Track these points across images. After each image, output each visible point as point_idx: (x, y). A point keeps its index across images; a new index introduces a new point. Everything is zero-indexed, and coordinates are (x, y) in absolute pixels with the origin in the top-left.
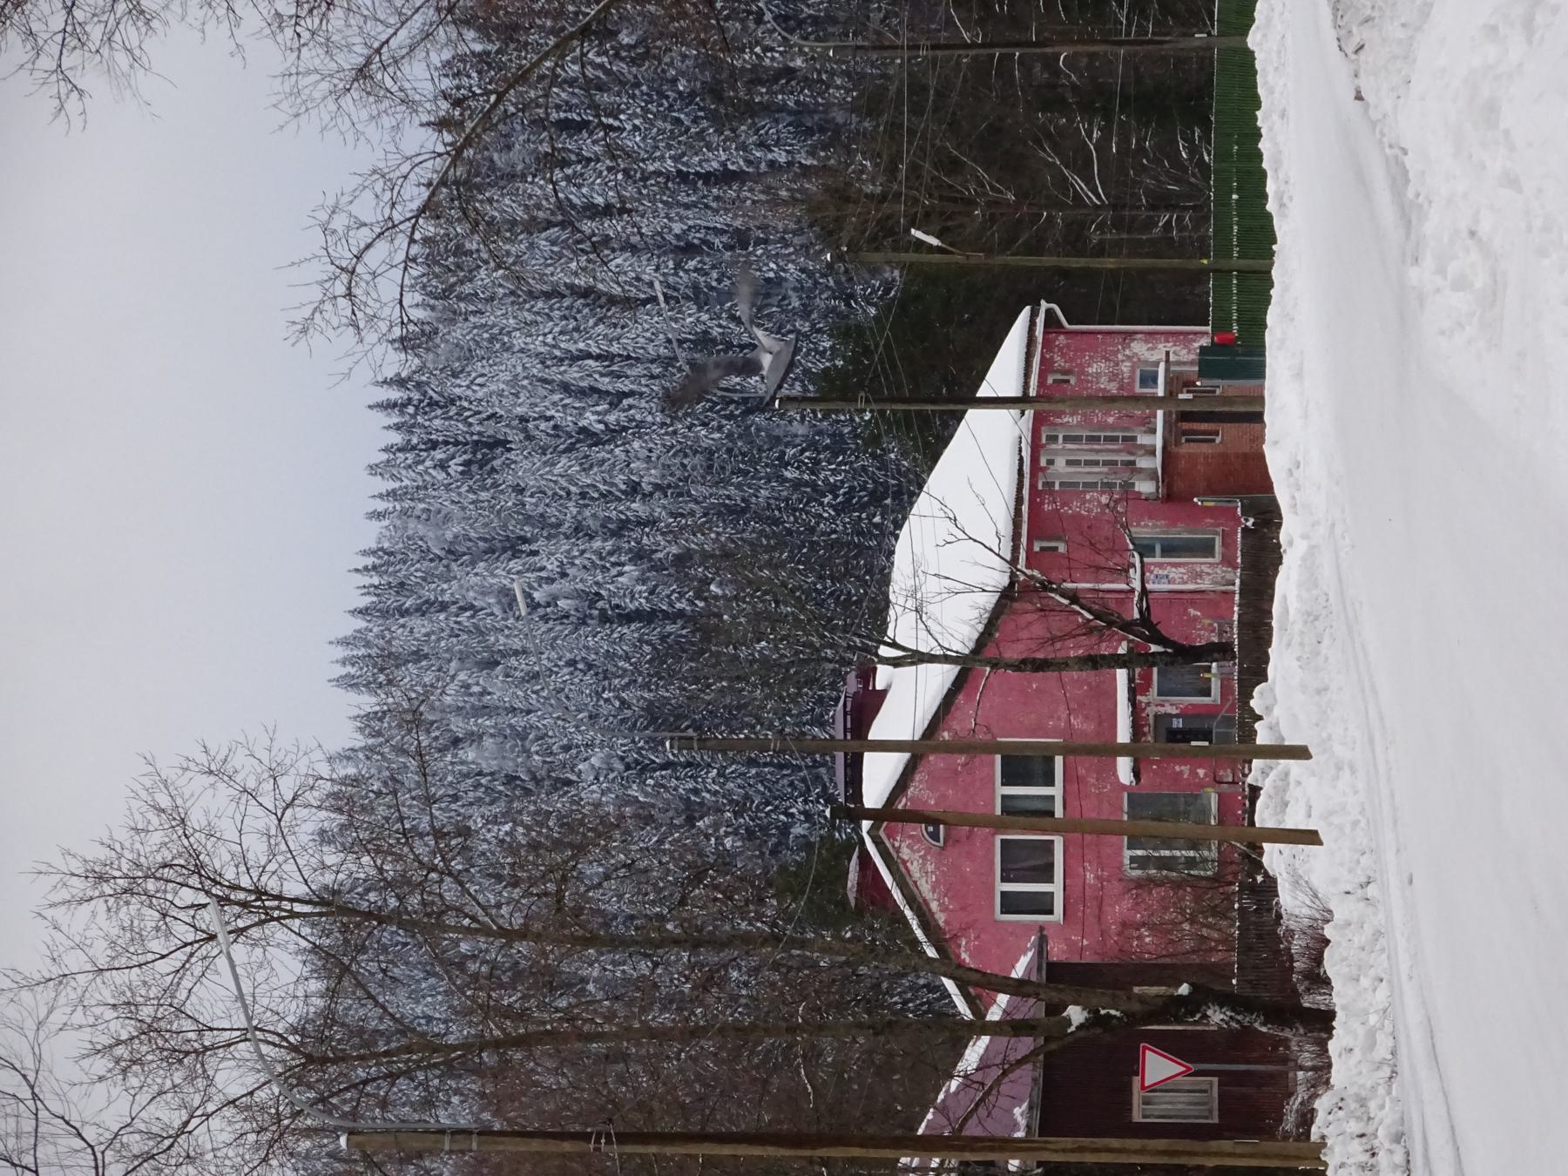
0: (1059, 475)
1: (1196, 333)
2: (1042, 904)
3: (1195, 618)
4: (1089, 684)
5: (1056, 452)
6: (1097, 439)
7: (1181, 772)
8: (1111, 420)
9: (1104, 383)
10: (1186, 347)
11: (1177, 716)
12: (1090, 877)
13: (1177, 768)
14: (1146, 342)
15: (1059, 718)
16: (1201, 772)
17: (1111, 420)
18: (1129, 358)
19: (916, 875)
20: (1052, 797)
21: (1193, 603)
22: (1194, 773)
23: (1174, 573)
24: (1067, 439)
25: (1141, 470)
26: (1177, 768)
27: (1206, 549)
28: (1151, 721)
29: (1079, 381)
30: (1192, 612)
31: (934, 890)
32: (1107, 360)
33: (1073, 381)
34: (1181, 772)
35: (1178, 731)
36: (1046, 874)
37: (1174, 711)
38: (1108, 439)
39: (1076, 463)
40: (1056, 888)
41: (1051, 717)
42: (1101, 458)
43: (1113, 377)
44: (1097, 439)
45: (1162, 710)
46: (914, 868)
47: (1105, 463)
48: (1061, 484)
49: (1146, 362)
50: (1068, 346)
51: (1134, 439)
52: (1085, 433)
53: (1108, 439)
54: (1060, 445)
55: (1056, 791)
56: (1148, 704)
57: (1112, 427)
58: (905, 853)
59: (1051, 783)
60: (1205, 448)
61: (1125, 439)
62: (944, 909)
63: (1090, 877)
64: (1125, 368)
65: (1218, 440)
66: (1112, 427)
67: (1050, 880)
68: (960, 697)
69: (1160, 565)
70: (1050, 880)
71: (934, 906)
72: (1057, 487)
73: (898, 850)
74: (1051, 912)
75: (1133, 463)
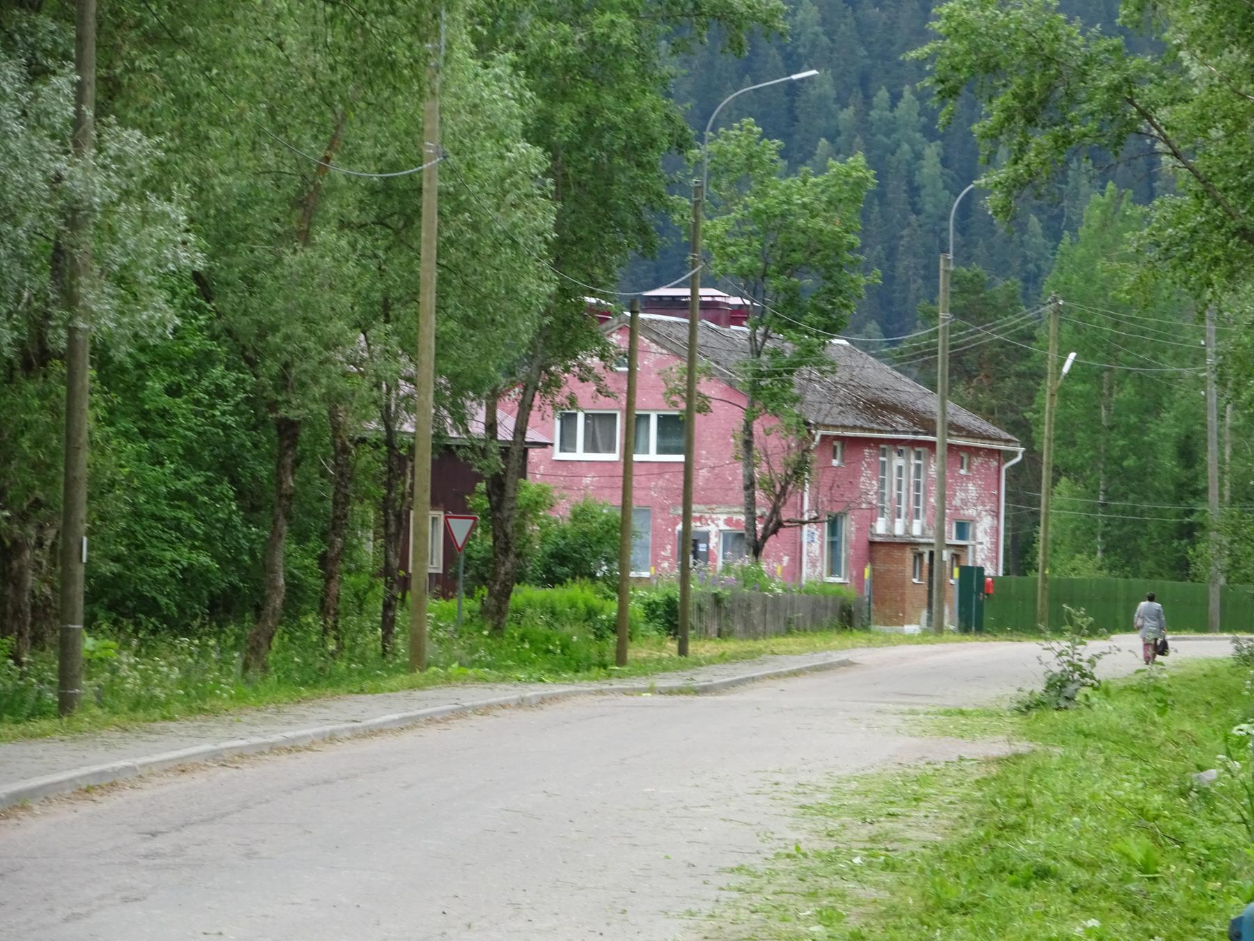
0: (890, 462)
1: (997, 565)
2: (567, 443)
3: (780, 561)
5: (909, 459)
6: (918, 489)
7: (664, 549)
8: (932, 500)
9: (960, 495)
10: (987, 558)
11: (708, 547)
12: (587, 481)
13: (669, 547)
14: (992, 527)
16: (666, 565)
17: (932, 500)
18: (979, 515)
20: (648, 452)
21: (792, 560)
22: (665, 558)
23: (816, 547)
24: (918, 467)
25: (893, 522)
26: (669, 547)
27: (833, 570)
28: (705, 529)
29: (962, 476)
30: (786, 559)
32: (978, 499)
33: (963, 472)
34: (664, 549)
36: (591, 446)
37: (711, 546)
38: (917, 497)
39: (900, 474)
40: (580, 454)
41: (708, 453)
42: (903, 493)
43: (965, 502)
44: (918, 489)
47: (899, 496)
48: (884, 462)
49: (975, 528)
50: (989, 468)
51: (918, 518)
52: (922, 480)
53: (917, 497)
54: (913, 461)
55: (653, 456)
57: (926, 501)
59: (661, 450)
60: (909, 570)
61: (918, 510)
63: (587, 481)
64: (971, 512)
65: (915, 580)
66: (926, 501)
67: (586, 450)
69: (821, 536)
70: (586, 450)
72: (882, 459)
74: (562, 450)
75: (899, 517)
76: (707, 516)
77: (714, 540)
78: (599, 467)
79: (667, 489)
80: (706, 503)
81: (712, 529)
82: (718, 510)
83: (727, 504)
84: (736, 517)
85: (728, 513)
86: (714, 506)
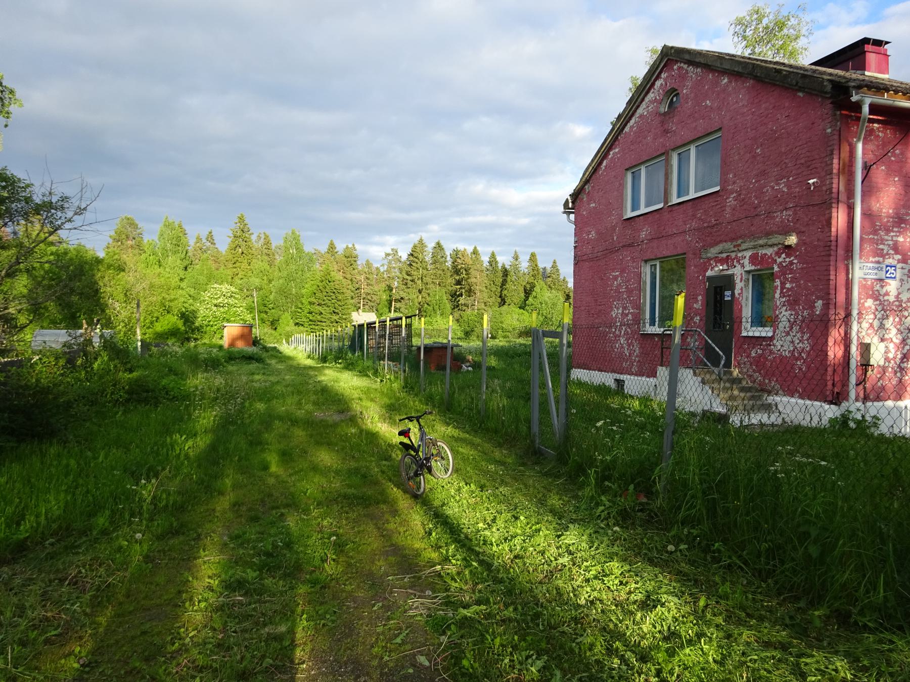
3: (812, 307)
4: (758, 206)
11: (733, 295)
12: (643, 235)
13: (700, 298)
15: (734, 183)
16: (697, 319)
19: (647, 100)
21: (826, 306)
26: (700, 298)
28: (730, 272)
30: (819, 304)
31: (641, 116)
35: (723, 296)
37: (737, 292)
40: (643, 210)
41: (735, 176)
45: (738, 281)
46: (651, 96)
56: (743, 266)
58: (658, 83)
62: (632, 127)
63: (643, 235)
68: (752, 81)
71: (632, 122)
73: (658, 77)
76: (733, 255)
77: (739, 285)
78: (650, 217)
79: (698, 230)
80: (732, 240)
81: (737, 271)
82: (743, 247)
83: (752, 236)
84: (762, 251)
85: (754, 247)
86: (739, 242)
